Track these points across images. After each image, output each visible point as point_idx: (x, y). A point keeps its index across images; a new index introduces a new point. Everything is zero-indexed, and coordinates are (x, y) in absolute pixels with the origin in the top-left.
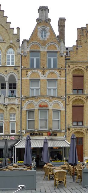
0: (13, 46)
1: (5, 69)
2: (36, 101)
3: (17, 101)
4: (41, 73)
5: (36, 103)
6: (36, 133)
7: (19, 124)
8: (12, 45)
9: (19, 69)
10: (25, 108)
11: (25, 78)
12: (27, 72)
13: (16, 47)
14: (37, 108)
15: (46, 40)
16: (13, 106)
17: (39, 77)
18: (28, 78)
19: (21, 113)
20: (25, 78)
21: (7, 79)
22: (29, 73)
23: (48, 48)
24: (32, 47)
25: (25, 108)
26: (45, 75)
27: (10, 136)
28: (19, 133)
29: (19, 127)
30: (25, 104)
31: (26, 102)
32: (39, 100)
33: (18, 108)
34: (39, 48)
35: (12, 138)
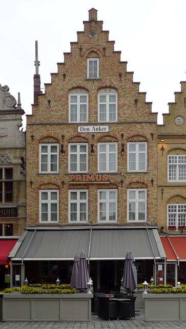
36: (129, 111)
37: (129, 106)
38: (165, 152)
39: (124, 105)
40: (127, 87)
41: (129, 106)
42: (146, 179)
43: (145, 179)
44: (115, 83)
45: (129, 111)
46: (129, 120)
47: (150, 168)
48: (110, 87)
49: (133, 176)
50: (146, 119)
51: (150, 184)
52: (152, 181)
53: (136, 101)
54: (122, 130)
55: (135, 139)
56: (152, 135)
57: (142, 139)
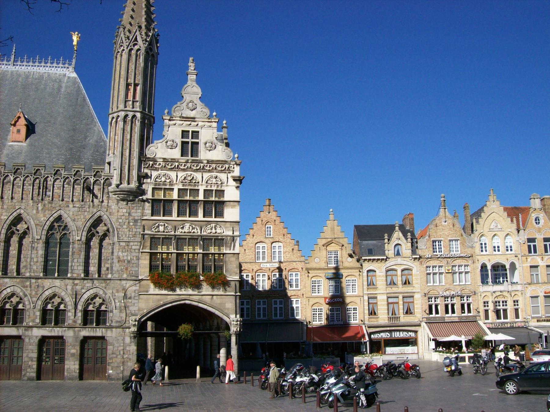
0: (512, 234)
1: (506, 257)
2: (540, 287)
3: (519, 287)
4: (540, 259)
5: (541, 289)
6: (544, 319)
7: (524, 310)
8: (510, 233)
9: (519, 256)
10: (529, 294)
11: (526, 265)
12: (527, 258)
13: (514, 235)
14: (542, 294)
15: (541, 227)
16: (516, 293)
17: (538, 263)
18: (529, 265)
19: (525, 298)
20: (526, 265)
21: (508, 267)
22: (529, 260)
23: (544, 235)
24: (528, 234)
25: (529, 294)
26: (544, 261)
27: (516, 322)
28: (525, 320)
29: (524, 313)
30: (528, 290)
31: (530, 288)
32: (544, 287)
33: (522, 294)
34: (535, 235)
35: (519, 325)
36: (289, 255)
37: (289, 252)
38: (310, 278)
39: (286, 252)
40: (288, 241)
41: (289, 252)
42: (299, 293)
43: (299, 293)
44: (281, 240)
45: (289, 255)
46: (289, 260)
47: (301, 287)
48: (278, 242)
49: (292, 292)
50: (299, 260)
51: (302, 296)
52: (303, 295)
53: (293, 249)
54: (285, 266)
55: (293, 270)
56: (302, 268)
57: (296, 270)
